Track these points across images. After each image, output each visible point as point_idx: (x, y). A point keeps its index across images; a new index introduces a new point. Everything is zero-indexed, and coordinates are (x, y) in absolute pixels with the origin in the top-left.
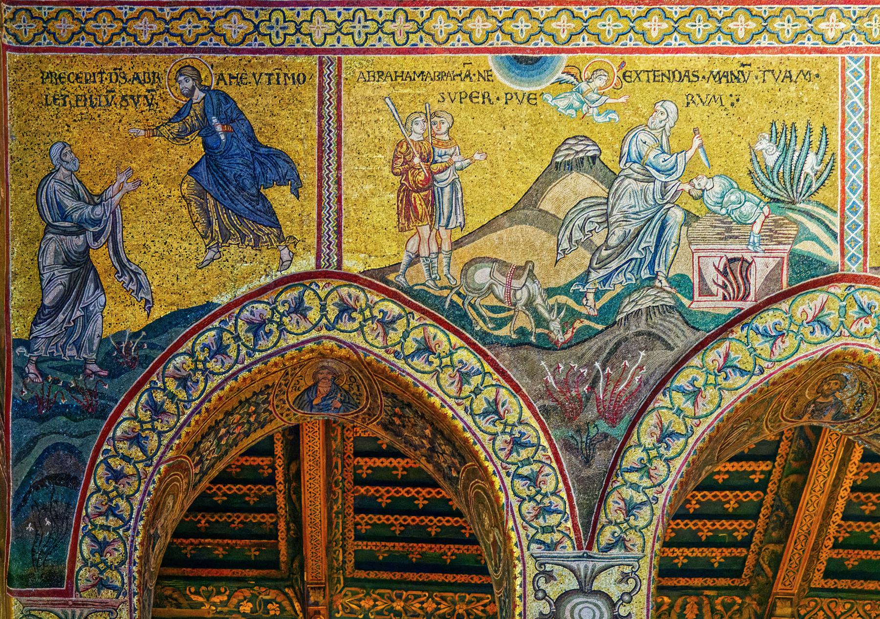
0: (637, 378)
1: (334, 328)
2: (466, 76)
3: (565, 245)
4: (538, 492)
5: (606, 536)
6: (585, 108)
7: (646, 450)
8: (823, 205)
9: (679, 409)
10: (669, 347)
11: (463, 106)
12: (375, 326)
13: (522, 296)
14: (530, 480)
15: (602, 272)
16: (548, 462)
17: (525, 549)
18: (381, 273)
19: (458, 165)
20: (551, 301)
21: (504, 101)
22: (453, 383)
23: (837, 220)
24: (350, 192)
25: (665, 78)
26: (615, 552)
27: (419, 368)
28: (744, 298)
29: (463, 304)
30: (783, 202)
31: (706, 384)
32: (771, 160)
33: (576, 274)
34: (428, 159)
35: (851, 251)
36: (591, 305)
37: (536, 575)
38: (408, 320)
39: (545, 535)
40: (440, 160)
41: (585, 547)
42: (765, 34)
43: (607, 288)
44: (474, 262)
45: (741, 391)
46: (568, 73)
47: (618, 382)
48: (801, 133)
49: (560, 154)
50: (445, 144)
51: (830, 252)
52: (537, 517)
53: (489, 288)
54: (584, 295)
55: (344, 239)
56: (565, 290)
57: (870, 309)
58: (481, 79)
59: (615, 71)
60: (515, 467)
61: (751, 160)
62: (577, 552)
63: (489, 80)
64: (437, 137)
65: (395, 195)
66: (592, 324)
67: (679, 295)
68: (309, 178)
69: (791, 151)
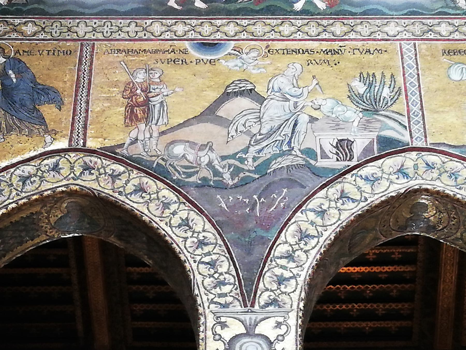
0: (282, 204)
1: (78, 179)
2: (172, 52)
3: (233, 133)
4: (216, 272)
5: (264, 298)
6: (245, 66)
7: (291, 245)
8: (396, 112)
9: (312, 221)
10: (303, 187)
11: (169, 65)
12: (107, 178)
13: (205, 160)
14: (211, 265)
15: (258, 147)
16: (224, 254)
17: (206, 308)
18: (112, 149)
19: (165, 94)
20: (225, 162)
21: (195, 63)
22: (158, 209)
23: (406, 120)
24: (95, 107)
25: (293, 53)
26: (271, 308)
27: (135, 201)
28: (350, 160)
29: (166, 164)
30: (371, 111)
31: (329, 207)
32: (361, 91)
33: (241, 148)
34: (146, 91)
35: (415, 135)
36: (250, 165)
37: (214, 325)
38: (129, 174)
39: (221, 298)
40: (153, 91)
41: (249, 306)
42: (352, 32)
43: (261, 155)
44: (173, 142)
45: (353, 211)
46: (235, 50)
47: (270, 207)
48: (378, 77)
49: (230, 88)
50: (157, 84)
51: (403, 135)
52: (215, 287)
53: (183, 156)
54: (246, 159)
55: (88, 131)
56: (233, 156)
57: (433, 165)
58: (181, 53)
59: (263, 49)
60: (200, 257)
61: (349, 91)
62: (243, 309)
63: (186, 53)
64: (152, 80)
65: (124, 109)
66: (251, 175)
67: (308, 159)
68: (68, 101)
69: (373, 86)
